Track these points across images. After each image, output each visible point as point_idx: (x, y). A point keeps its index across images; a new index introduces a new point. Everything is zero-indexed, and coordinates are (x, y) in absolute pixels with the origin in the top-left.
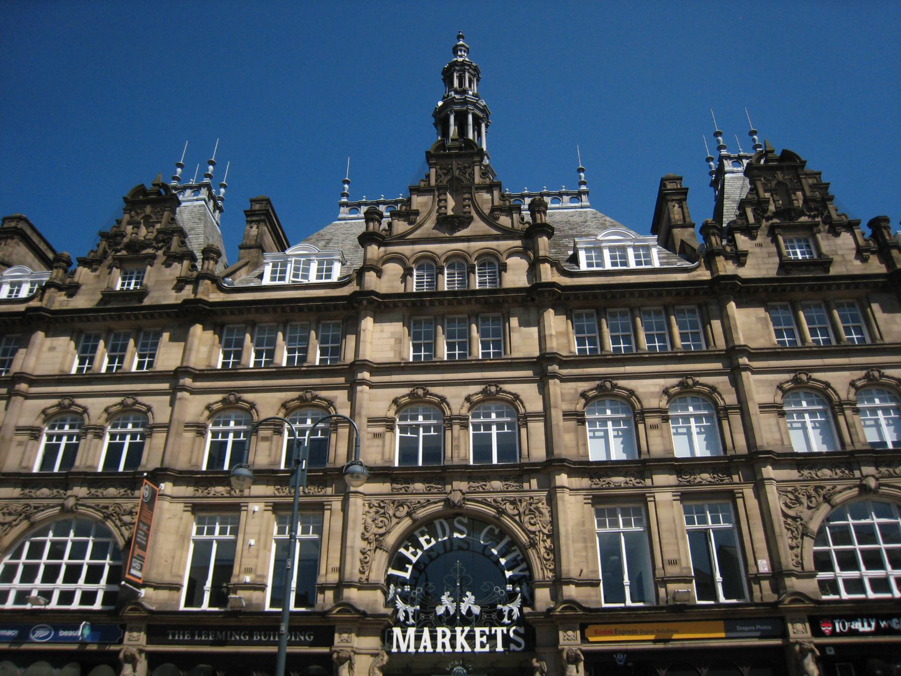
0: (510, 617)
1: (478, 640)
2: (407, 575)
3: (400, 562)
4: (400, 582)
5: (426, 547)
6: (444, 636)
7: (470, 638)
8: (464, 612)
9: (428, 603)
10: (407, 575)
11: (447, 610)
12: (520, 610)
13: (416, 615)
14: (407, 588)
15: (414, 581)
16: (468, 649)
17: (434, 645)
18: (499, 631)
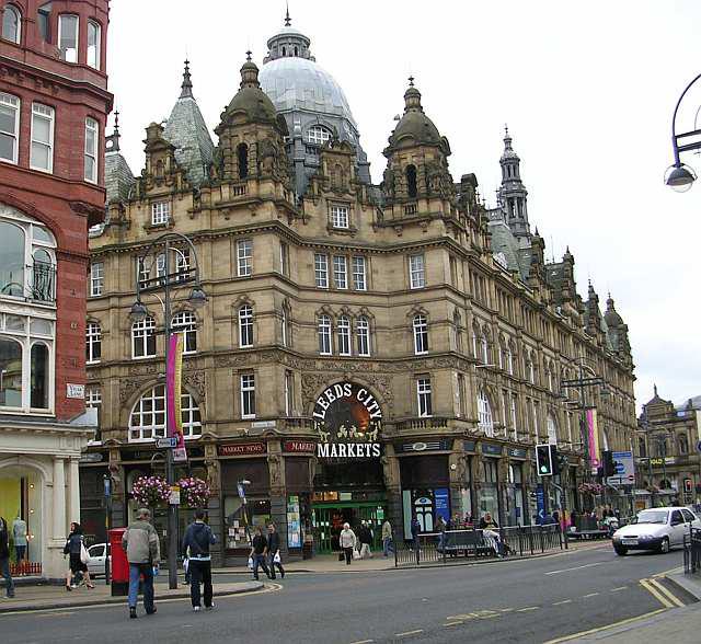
3: (319, 409)
7: (355, 450)
9: (334, 430)
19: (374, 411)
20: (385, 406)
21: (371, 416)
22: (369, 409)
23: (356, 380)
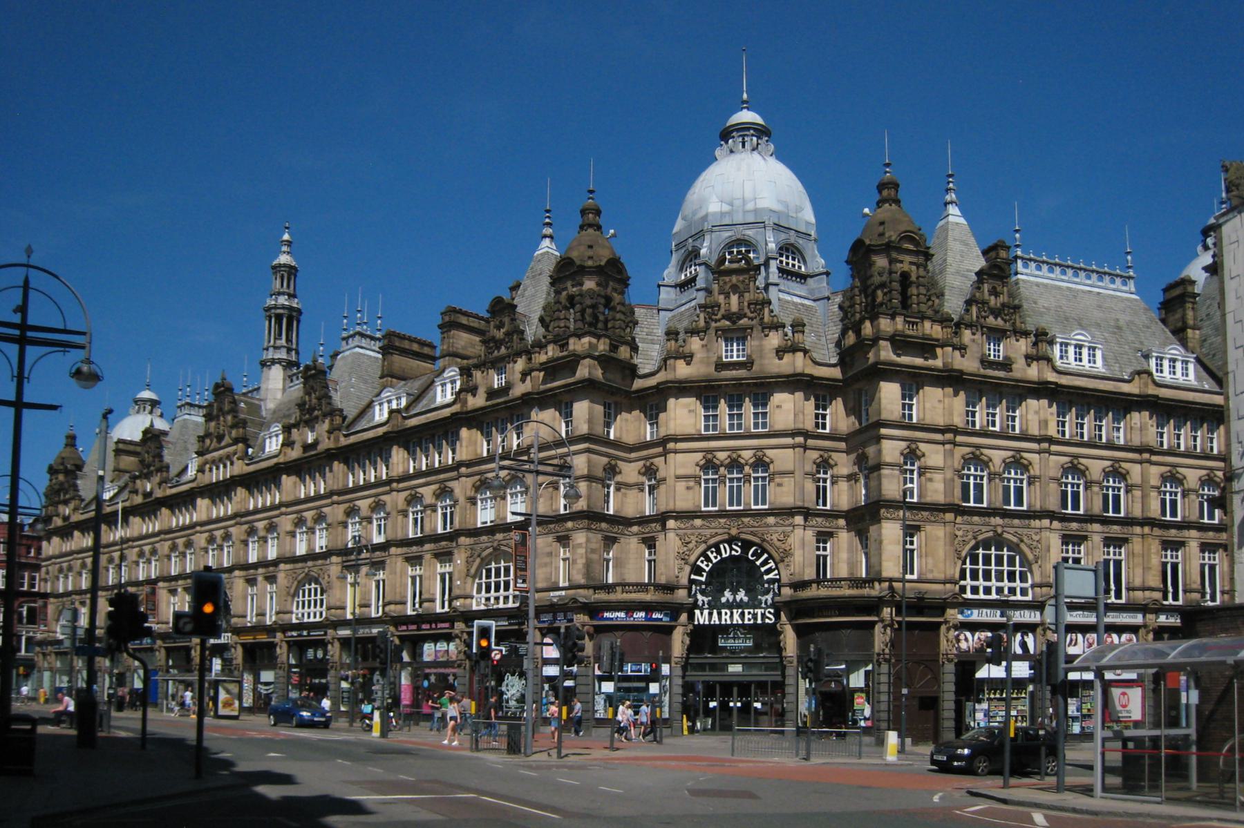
0: (766, 603)
1: (747, 616)
2: (703, 579)
3: (697, 570)
4: (701, 583)
5: (714, 561)
6: (726, 614)
7: (742, 615)
8: (738, 600)
10: (703, 579)
11: (728, 600)
12: (772, 599)
13: (709, 603)
14: (703, 587)
15: (706, 583)
16: (740, 622)
17: (720, 619)
18: (759, 611)
19: (769, 571)
20: (781, 565)
21: (766, 577)
22: (763, 569)
23: (743, 536)
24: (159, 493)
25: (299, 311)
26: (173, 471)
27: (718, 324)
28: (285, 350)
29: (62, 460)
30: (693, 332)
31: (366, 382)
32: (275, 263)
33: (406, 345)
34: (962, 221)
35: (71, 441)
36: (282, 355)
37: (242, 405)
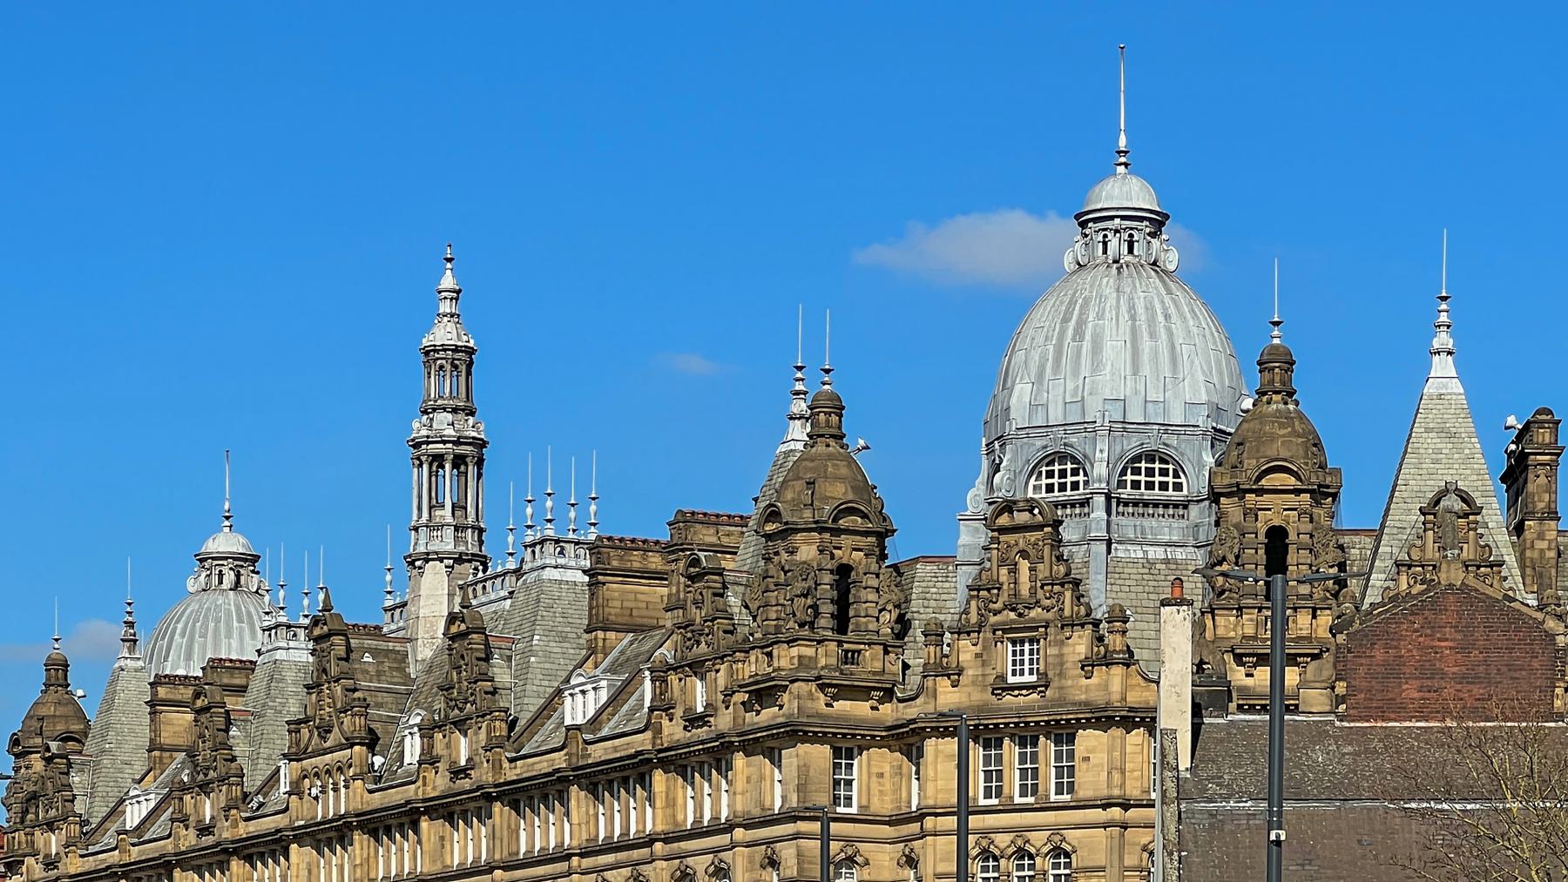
24: (225, 832)
25: (481, 444)
26: (252, 782)
27: (998, 618)
28: (450, 532)
29: (36, 722)
30: (960, 631)
31: (563, 638)
32: (425, 342)
33: (635, 561)
34: (1457, 387)
35: (58, 671)
36: (446, 543)
37: (368, 658)
